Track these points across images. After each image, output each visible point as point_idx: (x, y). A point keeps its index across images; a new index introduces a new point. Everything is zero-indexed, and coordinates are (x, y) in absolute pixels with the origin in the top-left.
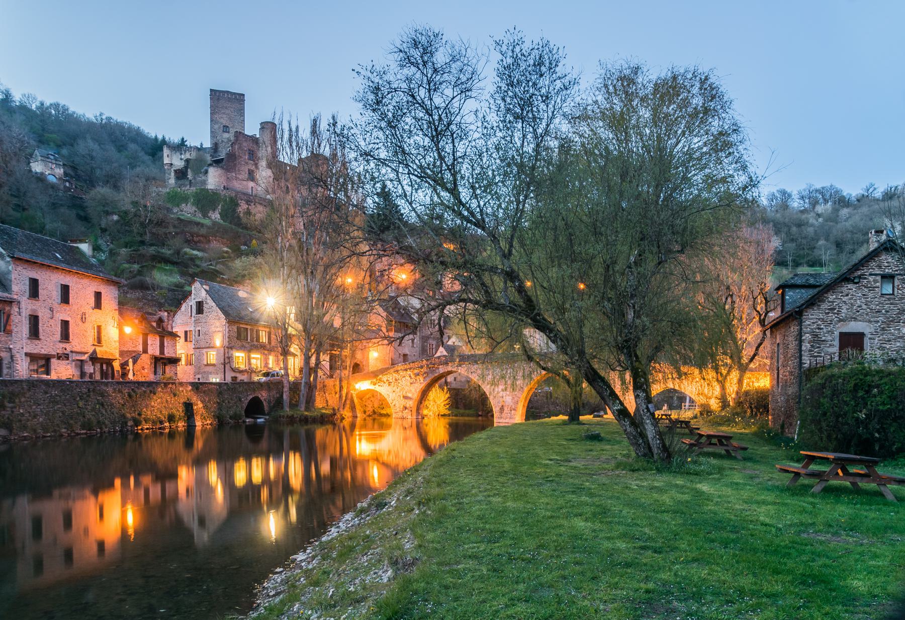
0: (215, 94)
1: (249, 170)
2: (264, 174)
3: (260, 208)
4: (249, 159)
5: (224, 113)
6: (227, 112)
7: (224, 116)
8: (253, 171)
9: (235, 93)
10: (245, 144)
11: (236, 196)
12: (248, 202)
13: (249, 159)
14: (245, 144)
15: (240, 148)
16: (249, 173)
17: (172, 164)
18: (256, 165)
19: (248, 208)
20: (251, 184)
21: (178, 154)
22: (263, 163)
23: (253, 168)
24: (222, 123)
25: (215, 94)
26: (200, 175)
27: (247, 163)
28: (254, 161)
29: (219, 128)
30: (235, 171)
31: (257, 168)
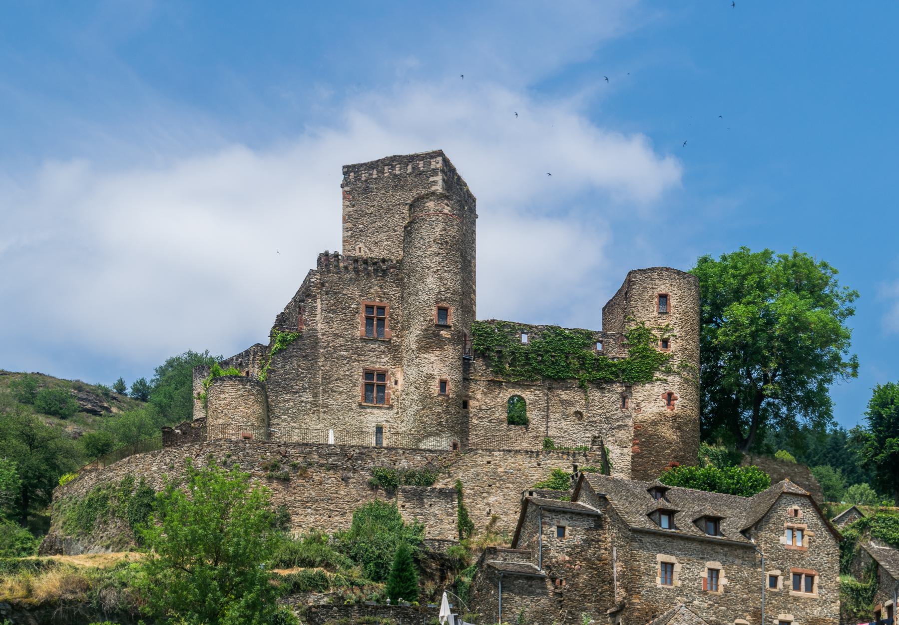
1: (368, 374)
2: (413, 372)
5: (379, 230)
8: (382, 375)
14: (350, 291)
18: (395, 353)
20: (374, 417)
23: (383, 363)
25: (358, 178)
27: (358, 351)
31: (397, 359)
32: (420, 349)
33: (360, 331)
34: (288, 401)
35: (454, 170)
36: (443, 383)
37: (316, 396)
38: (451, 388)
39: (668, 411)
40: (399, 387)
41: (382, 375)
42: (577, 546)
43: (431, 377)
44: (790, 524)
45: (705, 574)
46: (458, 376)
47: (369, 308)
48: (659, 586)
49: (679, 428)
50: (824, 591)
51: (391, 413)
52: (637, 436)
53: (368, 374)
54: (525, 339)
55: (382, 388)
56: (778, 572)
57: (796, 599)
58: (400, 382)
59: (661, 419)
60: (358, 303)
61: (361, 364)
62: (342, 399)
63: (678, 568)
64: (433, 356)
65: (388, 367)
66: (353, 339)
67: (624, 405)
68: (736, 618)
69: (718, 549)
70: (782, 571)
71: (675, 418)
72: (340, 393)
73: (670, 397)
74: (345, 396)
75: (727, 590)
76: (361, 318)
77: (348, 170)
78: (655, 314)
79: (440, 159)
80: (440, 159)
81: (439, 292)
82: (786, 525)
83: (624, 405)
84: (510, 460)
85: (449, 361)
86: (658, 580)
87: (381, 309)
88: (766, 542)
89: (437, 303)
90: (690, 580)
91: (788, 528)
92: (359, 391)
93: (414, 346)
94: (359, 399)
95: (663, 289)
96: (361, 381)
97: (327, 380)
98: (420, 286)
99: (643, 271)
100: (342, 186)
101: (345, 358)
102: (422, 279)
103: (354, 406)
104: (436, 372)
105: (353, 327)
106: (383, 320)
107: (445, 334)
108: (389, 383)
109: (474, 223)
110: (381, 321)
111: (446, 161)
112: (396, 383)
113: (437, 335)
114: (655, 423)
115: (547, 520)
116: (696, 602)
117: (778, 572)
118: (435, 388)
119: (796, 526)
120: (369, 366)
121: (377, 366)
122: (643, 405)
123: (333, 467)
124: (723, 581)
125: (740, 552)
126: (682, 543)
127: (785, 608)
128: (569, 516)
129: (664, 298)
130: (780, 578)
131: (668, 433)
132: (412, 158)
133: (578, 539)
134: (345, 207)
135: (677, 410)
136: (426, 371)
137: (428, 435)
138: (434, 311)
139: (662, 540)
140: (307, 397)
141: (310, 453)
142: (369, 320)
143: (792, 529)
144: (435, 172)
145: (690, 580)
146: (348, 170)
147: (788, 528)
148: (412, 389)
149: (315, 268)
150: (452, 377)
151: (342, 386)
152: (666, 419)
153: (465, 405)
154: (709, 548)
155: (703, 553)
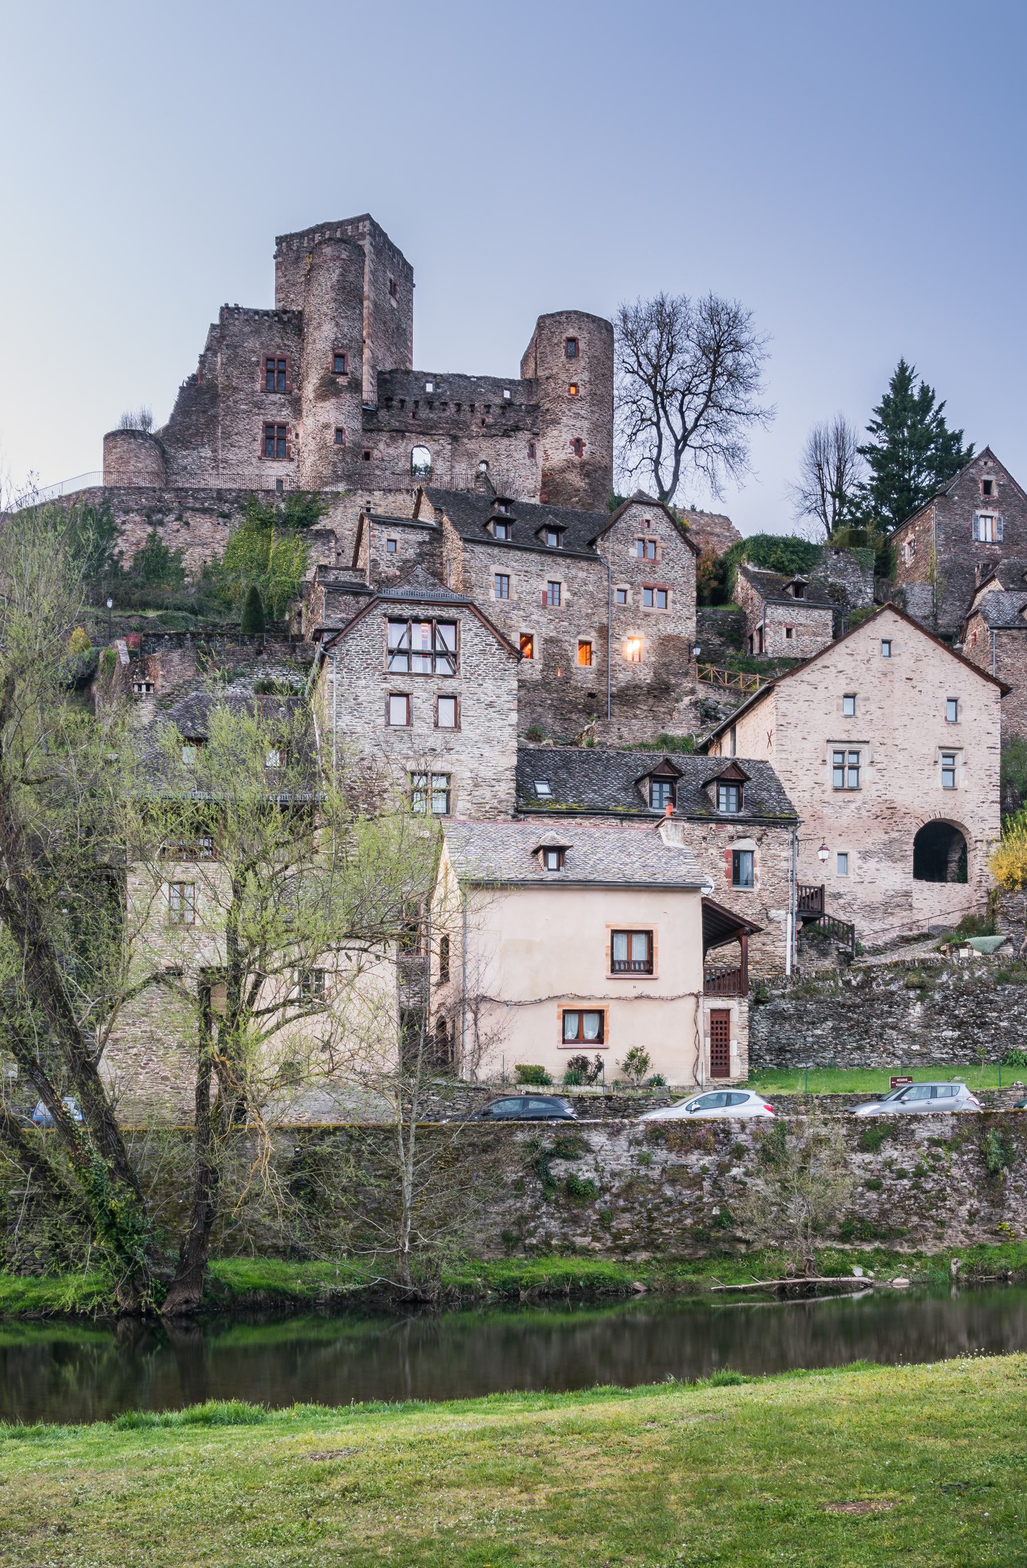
1: (268, 426)
3: (204, 525)
4: (267, 390)
11: (106, 502)
12: (153, 515)
13: (267, 390)
14: (252, 343)
15: (229, 362)
16: (268, 438)
18: (296, 405)
19: (152, 537)
20: (276, 470)
22: (309, 390)
23: (284, 415)
27: (259, 405)
28: (288, 392)
30: (213, 440)
31: (298, 413)
34: (186, 457)
35: (385, 235)
36: (339, 431)
37: (214, 451)
38: (348, 438)
39: (576, 459)
40: (300, 441)
41: (283, 427)
42: (408, 561)
43: (326, 426)
44: (641, 536)
45: (545, 587)
46: (357, 425)
48: (493, 599)
49: (587, 475)
50: (678, 607)
51: (292, 466)
52: (544, 484)
53: (268, 426)
54: (430, 388)
55: (283, 439)
56: (627, 586)
57: (647, 615)
58: (301, 435)
59: (570, 465)
60: (258, 356)
61: (261, 417)
62: (242, 454)
63: (514, 580)
64: (330, 404)
67: (532, 455)
68: (579, 633)
69: (560, 560)
70: (632, 584)
71: (583, 465)
72: (240, 447)
73: (578, 444)
74: (245, 451)
75: (569, 604)
77: (280, 240)
78: (563, 358)
79: (367, 223)
80: (367, 223)
81: (336, 339)
82: (636, 536)
83: (532, 455)
84: (391, 498)
85: (345, 409)
86: (493, 594)
88: (614, 554)
89: (333, 349)
90: (528, 593)
91: (640, 540)
92: (258, 446)
93: (311, 396)
95: (571, 333)
96: (260, 436)
97: (226, 435)
99: (552, 315)
100: (275, 257)
101: (245, 412)
103: (254, 460)
104: (332, 421)
105: (253, 380)
106: (284, 372)
107: (342, 381)
108: (291, 437)
109: (411, 292)
111: (375, 225)
112: (297, 435)
113: (333, 382)
114: (563, 471)
115: (376, 533)
116: (534, 617)
117: (627, 586)
118: (330, 435)
119: (647, 537)
120: (270, 419)
121: (278, 419)
122: (549, 452)
124: (566, 595)
125: (584, 564)
126: (519, 553)
127: (634, 624)
128: (400, 529)
130: (630, 593)
131: (575, 479)
132: (341, 224)
133: (411, 553)
134: (277, 278)
135: (586, 456)
136: (323, 419)
137: (326, 484)
138: (330, 359)
139: (496, 551)
140: (207, 452)
141: (186, 497)
143: (642, 540)
144: (363, 236)
145: (528, 593)
146: (280, 240)
147: (640, 540)
149: (217, 322)
150: (354, 424)
151: (243, 441)
152: (574, 466)
153: (367, 456)
154: (549, 560)
155: (542, 564)
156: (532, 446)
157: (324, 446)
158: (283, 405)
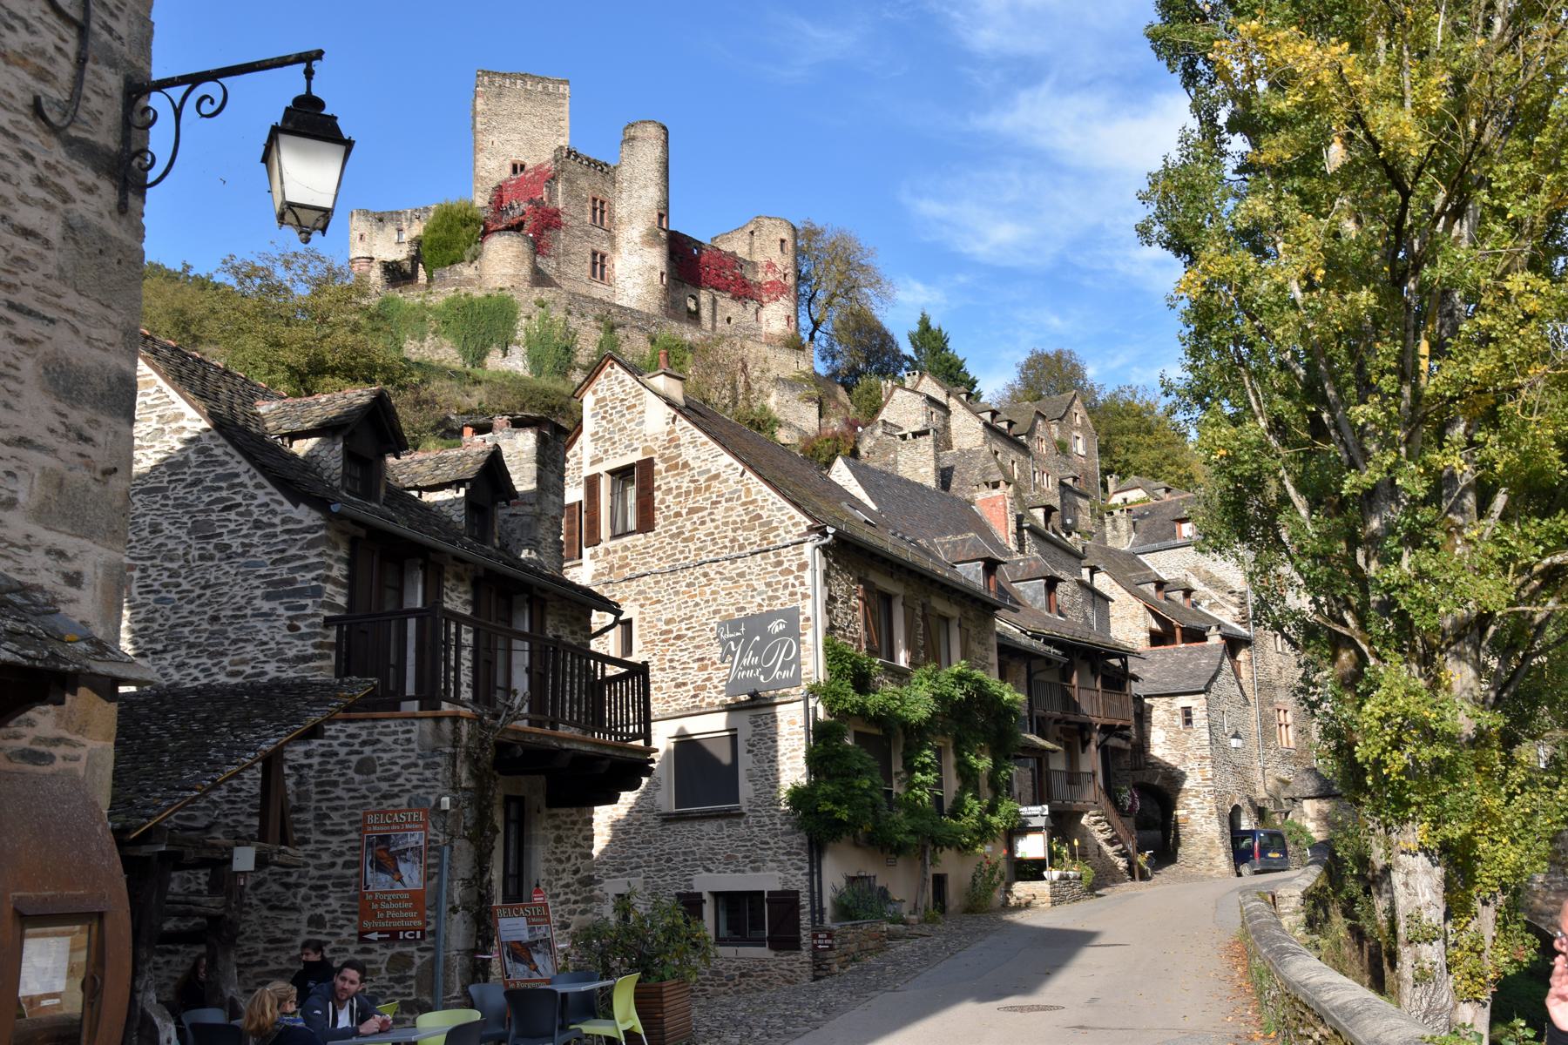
0: (492, 82)
1: (594, 254)
2: (636, 261)
6: (522, 125)
7: (516, 137)
8: (603, 257)
9: (543, 79)
10: (583, 182)
14: (583, 182)
16: (594, 263)
17: (372, 259)
18: (612, 239)
21: (390, 229)
23: (604, 247)
24: (507, 156)
25: (492, 82)
26: (458, 267)
27: (588, 234)
29: (501, 167)
31: (614, 247)
32: (642, 243)
33: (588, 218)
36: (662, 274)
37: (558, 264)
43: (653, 268)
47: (595, 200)
51: (612, 289)
55: (603, 266)
65: (608, 251)
66: (584, 222)
76: (589, 206)
87: (602, 203)
92: (588, 267)
93: (638, 240)
94: (589, 274)
96: (589, 259)
98: (642, 192)
102: (645, 186)
103: (585, 279)
108: (608, 266)
110: (602, 212)
121: (601, 249)
123: (641, 329)
129: (783, 241)
138: (656, 215)
142: (595, 209)
148: (636, 274)
156: (757, 313)
157: (651, 284)
158: (604, 238)
